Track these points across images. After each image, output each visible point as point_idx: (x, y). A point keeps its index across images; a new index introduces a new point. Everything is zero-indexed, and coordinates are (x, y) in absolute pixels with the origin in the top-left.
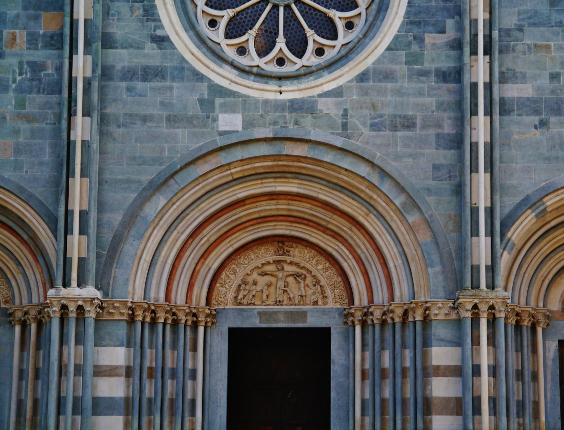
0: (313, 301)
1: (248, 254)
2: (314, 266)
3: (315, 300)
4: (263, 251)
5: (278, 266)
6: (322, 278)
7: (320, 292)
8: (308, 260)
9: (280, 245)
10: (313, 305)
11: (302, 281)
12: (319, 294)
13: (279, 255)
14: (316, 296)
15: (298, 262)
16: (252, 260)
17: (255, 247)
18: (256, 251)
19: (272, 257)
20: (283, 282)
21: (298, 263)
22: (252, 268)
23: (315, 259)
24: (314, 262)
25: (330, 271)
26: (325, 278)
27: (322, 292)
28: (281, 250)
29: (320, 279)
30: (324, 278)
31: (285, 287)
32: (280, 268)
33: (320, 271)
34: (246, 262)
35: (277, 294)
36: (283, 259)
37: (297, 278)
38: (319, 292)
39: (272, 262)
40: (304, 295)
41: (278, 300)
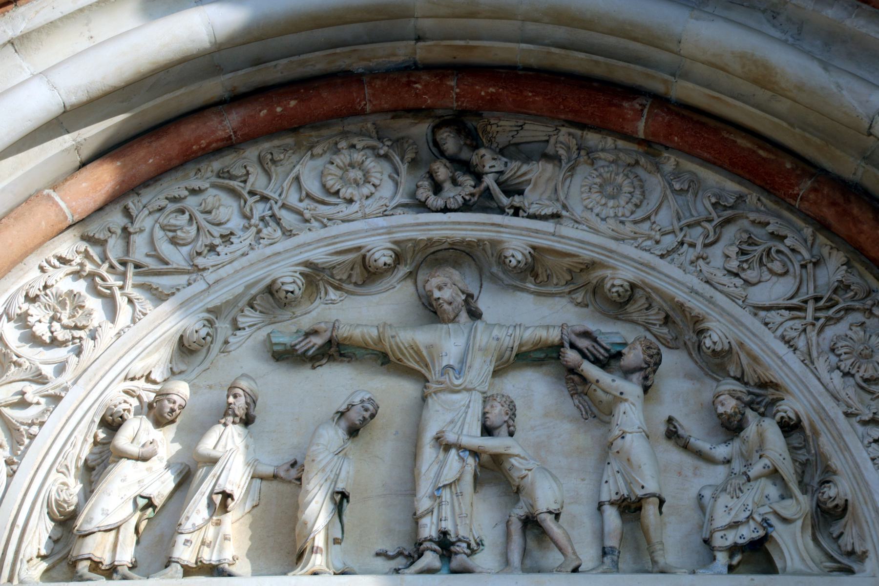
0: (731, 538)
1: (192, 202)
2: (720, 277)
3: (747, 533)
4: (313, 187)
5: (434, 282)
6: (793, 360)
7: (788, 470)
8: (669, 241)
9: (450, 142)
10: (731, 569)
11: (632, 389)
12: (773, 491)
13: (445, 210)
14: (750, 496)
15: (587, 254)
16: (227, 238)
17: (251, 153)
18: (257, 180)
19: (382, 222)
20: (477, 398)
21: (591, 266)
22: (215, 299)
23: (730, 232)
24: (716, 251)
25: (858, 317)
26: (821, 365)
27: (803, 468)
28: (455, 182)
29: (777, 374)
30: (808, 360)
31: (487, 431)
32: (446, 294)
33: (774, 317)
34: (177, 257)
35: (425, 488)
36: (472, 235)
37: (591, 370)
38: (774, 474)
39: (382, 257)
40: (651, 486)
41: (429, 529)
